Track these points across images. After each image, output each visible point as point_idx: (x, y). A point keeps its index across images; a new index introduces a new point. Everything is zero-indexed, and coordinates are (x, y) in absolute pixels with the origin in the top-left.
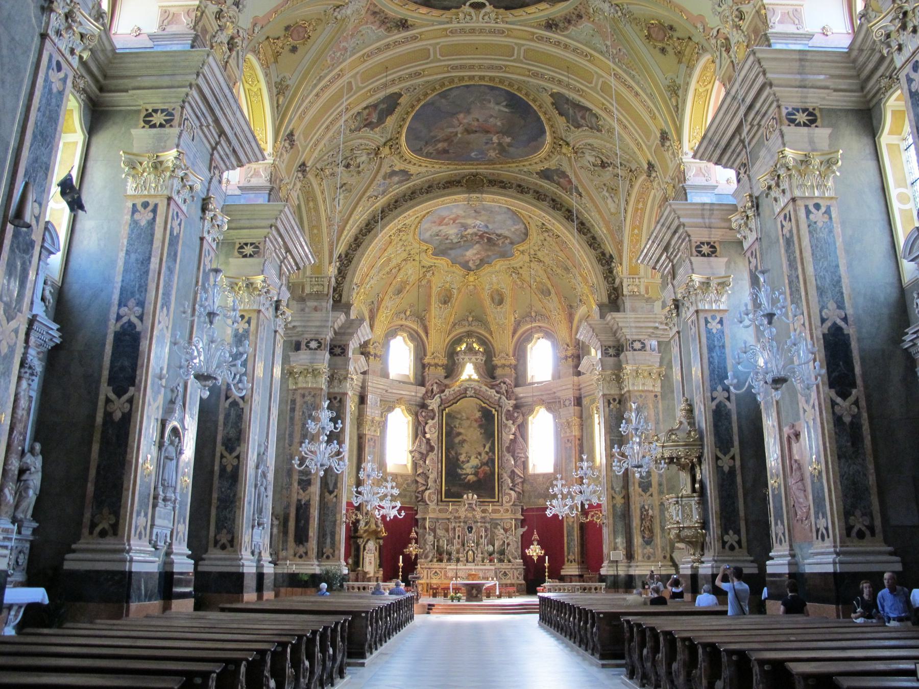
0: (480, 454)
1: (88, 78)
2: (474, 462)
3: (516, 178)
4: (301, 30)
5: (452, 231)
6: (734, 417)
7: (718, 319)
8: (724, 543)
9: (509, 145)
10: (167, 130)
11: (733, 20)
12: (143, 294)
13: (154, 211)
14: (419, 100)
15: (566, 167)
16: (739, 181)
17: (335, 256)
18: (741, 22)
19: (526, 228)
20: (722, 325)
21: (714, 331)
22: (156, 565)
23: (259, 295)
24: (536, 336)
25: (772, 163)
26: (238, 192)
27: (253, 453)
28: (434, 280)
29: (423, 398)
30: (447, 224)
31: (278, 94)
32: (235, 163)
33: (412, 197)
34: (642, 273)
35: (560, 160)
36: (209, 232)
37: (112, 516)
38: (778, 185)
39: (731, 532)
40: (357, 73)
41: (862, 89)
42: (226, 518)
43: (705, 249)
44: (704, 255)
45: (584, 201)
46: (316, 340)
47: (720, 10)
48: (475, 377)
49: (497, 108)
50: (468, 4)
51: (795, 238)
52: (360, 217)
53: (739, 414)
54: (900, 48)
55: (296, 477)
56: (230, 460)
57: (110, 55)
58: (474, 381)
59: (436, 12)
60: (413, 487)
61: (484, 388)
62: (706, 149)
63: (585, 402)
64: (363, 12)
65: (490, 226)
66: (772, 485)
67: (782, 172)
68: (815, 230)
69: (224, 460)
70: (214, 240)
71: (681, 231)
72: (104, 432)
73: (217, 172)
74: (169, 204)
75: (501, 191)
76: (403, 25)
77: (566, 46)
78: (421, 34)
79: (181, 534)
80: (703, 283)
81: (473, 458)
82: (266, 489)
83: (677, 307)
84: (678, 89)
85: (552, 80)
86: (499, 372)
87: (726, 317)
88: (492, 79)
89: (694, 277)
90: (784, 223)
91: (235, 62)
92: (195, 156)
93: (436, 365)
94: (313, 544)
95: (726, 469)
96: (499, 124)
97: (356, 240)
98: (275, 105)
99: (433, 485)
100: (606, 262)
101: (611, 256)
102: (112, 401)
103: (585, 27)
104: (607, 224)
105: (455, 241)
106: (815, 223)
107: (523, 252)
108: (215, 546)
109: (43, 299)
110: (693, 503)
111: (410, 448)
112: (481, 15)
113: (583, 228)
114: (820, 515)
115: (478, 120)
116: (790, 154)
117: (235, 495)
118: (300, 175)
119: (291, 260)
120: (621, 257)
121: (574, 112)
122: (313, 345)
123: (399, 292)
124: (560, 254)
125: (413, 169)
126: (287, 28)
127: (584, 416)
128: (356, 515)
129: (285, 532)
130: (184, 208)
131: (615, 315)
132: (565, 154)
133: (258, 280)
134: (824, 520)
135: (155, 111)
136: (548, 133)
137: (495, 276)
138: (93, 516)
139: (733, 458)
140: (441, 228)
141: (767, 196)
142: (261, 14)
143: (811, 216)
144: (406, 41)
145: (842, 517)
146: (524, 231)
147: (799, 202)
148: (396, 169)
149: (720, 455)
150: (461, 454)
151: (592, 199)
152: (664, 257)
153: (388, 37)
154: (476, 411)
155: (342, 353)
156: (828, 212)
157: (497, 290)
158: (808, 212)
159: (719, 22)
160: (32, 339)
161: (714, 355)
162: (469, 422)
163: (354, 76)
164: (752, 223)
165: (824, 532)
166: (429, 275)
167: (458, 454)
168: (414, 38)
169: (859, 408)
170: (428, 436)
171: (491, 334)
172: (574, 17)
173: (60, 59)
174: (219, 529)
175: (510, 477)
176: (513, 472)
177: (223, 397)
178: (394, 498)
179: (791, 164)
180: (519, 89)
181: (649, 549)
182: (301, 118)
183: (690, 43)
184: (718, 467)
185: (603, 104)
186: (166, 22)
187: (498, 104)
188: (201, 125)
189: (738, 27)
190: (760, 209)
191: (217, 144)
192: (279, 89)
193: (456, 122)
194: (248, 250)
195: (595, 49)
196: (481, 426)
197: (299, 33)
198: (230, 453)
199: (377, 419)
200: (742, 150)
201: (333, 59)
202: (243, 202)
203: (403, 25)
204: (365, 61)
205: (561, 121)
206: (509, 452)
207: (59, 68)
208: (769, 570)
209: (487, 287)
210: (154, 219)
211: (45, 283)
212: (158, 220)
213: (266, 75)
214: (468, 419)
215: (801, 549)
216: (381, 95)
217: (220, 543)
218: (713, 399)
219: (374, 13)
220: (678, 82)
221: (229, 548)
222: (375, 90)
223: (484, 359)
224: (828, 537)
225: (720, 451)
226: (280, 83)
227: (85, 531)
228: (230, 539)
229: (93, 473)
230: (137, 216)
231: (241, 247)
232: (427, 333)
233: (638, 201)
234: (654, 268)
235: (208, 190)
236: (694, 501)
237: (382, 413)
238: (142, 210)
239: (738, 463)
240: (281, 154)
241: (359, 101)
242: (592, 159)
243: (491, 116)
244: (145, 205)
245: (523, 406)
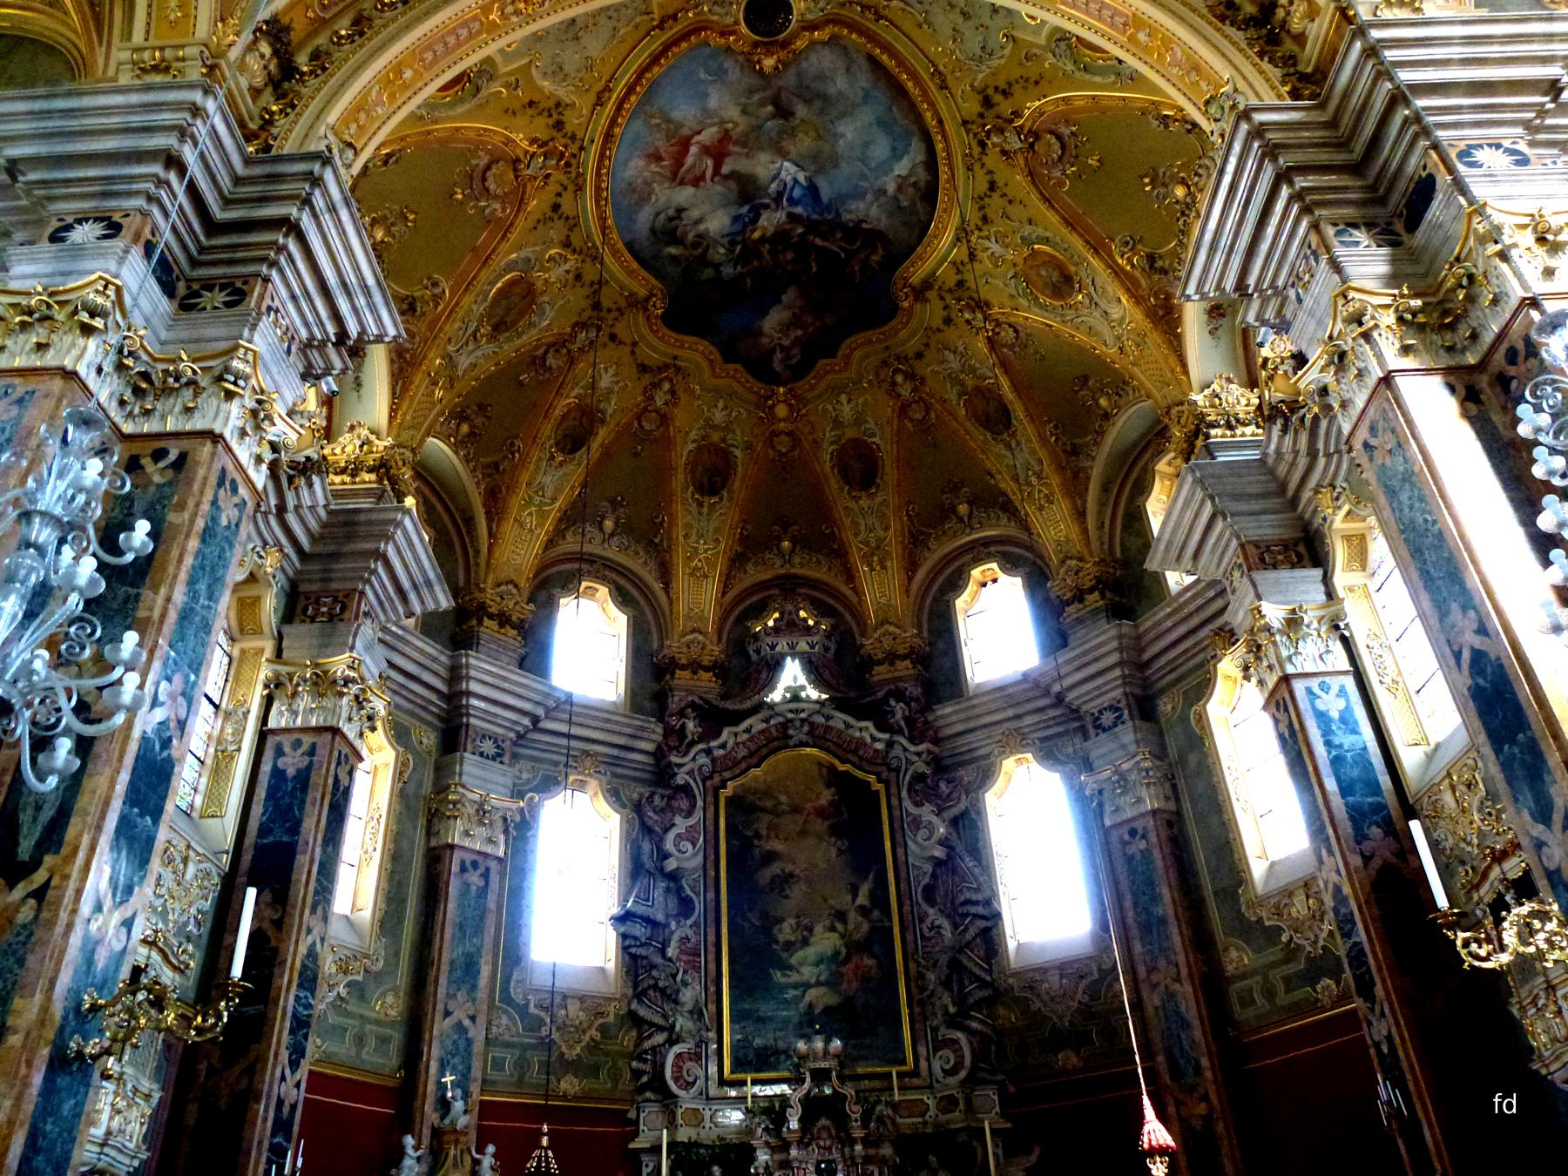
0: (841, 916)
2: (825, 942)
19: (931, 164)
24: (976, 573)
28: (680, 416)
29: (659, 754)
30: (697, 181)
48: (813, 694)
58: (808, 700)
60: (628, 1039)
61: (840, 719)
63: (1165, 706)
65: (826, 193)
81: (818, 929)
86: (881, 673)
93: (695, 666)
99: (689, 1025)
105: (728, 271)
111: (616, 910)
123: (572, 441)
127: (1173, 752)
137: (849, 403)
146: (922, 176)
150: (781, 920)
154: (820, 786)
157: (856, 443)
162: (800, 819)
167: (770, 922)
170: (671, 865)
171: (850, 576)
175: (946, 984)
176: (955, 966)
196: (835, 831)
199: (499, 801)
206: (932, 903)
209: (829, 435)
214: (796, 810)
223: (833, 647)
245: (962, 764)
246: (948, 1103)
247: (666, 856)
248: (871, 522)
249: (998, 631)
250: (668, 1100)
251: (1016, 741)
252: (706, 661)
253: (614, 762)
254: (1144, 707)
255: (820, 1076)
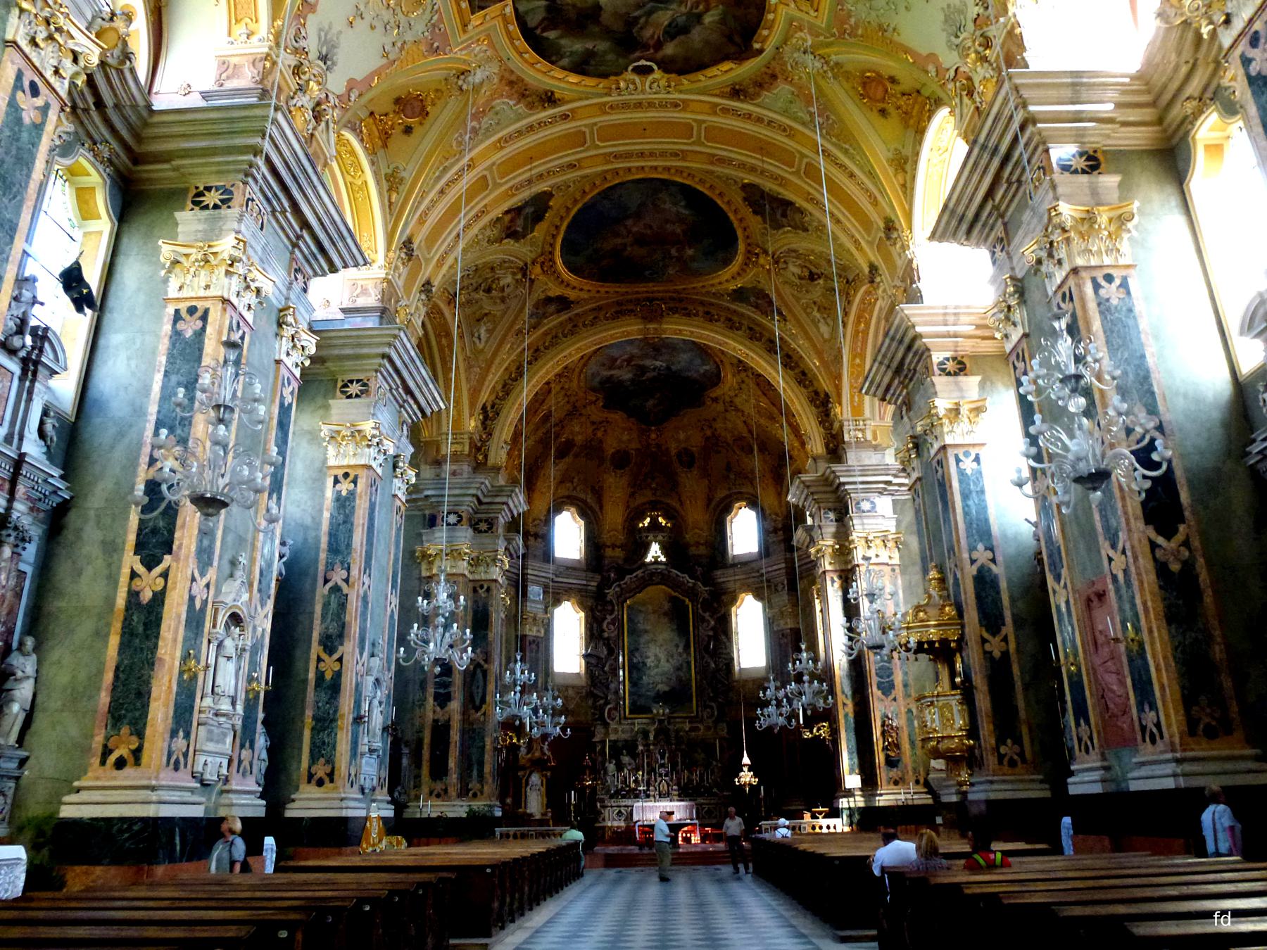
0: (672, 656)
1: (115, 145)
2: (666, 666)
3: (702, 303)
4: (417, 104)
5: (626, 375)
6: (1003, 585)
7: (973, 457)
8: (1001, 758)
9: (693, 259)
10: (224, 211)
11: (977, 52)
12: (186, 429)
13: (204, 318)
14: (576, 201)
15: (764, 284)
16: (994, 263)
17: (479, 406)
18: (987, 52)
20: (979, 463)
21: (969, 472)
22: (202, 808)
23: (369, 446)
25: (1040, 228)
26: (340, 316)
27: (361, 654)
29: (601, 587)
31: (390, 190)
32: (326, 267)
33: (573, 329)
34: (867, 413)
35: (756, 275)
36: (288, 354)
37: (134, 738)
38: (1050, 255)
39: (1009, 741)
40: (494, 164)
41: (1160, 121)
42: (324, 743)
43: (950, 366)
44: (949, 374)
45: (789, 326)
46: (455, 513)
47: (957, 41)
48: (663, 559)
49: (674, 209)
50: (630, 68)
51: (1081, 323)
52: (506, 358)
53: (1009, 581)
54: (1227, 21)
55: (431, 690)
56: (329, 666)
57: (145, 113)
58: (661, 563)
59: (590, 81)
62: (948, 223)
64: (496, 80)
66: (1068, 670)
67: (1057, 237)
68: (1108, 309)
69: (322, 664)
70: (297, 365)
71: (917, 344)
72: (127, 622)
73: (300, 277)
74: (225, 310)
75: (684, 320)
76: (549, 99)
77: (759, 120)
78: (572, 110)
79: (246, 763)
80: (950, 410)
82: (380, 703)
83: (916, 446)
84: (905, 163)
85: (742, 166)
87: (983, 453)
88: (668, 169)
89: (938, 402)
90: (1062, 305)
91: (324, 137)
92: (264, 249)
94: (453, 777)
95: (997, 654)
96: (679, 231)
97: (504, 387)
98: (387, 203)
100: (823, 404)
101: (827, 395)
102: (139, 576)
103: (782, 90)
104: (819, 354)
106: (1108, 300)
107: (715, 400)
108: (309, 782)
109: (42, 433)
110: (954, 703)
112: (648, 84)
113: (790, 361)
114: (1147, 708)
115: (651, 227)
116: (1067, 211)
117: (336, 712)
118: (423, 297)
119: (415, 407)
120: (839, 395)
121: (776, 210)
122: (453, 519)
124: (763, 398)
125: (572, 295)
126: (398, 101)
128: (511, 738)
129: (418, 765)
130: (249, 317)
131: (837, 468)
132: (763, 266)
133: (368, 427)
134: (1153, 714)
135: (208, 189)
136: (740, 241)
137: (682, 434)
138: (107, 739)
139: (1005, 639)
140: (612, 372)
141: (1035, 274)
142: (359, 76)
143: (1102, 292)
144: (554, 120)
145: (1181, 708)
147: (1083, 274)
148: (551, 294)
149: (986, 635)
151: (798, 321)
152: (896, 382)
153: (531, 115)
155: (490, 529)
156: (1124, 285)
158: (1097, 286)
159: (957, 59)
160: (21, 490)
161: (970, 503)
163: (490, 168)
164: (1017, 315)
165: (1155, 730)
166: (599, 434)
168: (565, 117)
169: (1190, 551)
170: (606, 635)
171: (682, 504)
172: (767, 79)
173: (37, 79)
174: (313, 759)
177: (320, 581)
178: (556, 713)
179: (1068, 224)
180: (702, 181)
181: (894, 773)
182: (421, 221)
183: (920, 99)
184: (985, 652)
185: (809, 194)
186: (224, 76)
187: (675, 204)
188: (274, 211)
189: (984, 59)
190: (1026, 296)
191: (299, 237)
192: (391, 182)
193: (623, 231)
194: (354, 389)
195: (795, 119)
196: (671, 620)
197: (413, 108)
198: (330, 655)
199: (541, 615)
200: (996, 220)
201: (459, 144)
202: (346, 327)
203: (549, 99)
204: (502, 148)
205: (755, 222)
207: (35, 91)
208: (1073, 790)
210: (204, 329)
211: (45, 413)
212: (209, 329)
213: (373, 163)
215: (1119, 758)
216: (525, 194)
217: (316, 777)
218: (973, 562)
219: (511, 83)
220: (904, 152)
221: (328, 785)
222: (517, 188)
224: (1162, 737)
225: (987, 631)
226: (392, 175)
227: (96, 761)
228: (328, 771)
229: (109, 677)
230: (180, 326)
231: (345, 386)
232: (601, 507)
233: (858, 322)
234: (883, 399)
235: (287, 299)
236: (954, 701)
237: (546, 607)
238: (188, 317)
239: (1012, 646)
240: (396, 268)
241: (498, 202)
242: (797, 271)
243: (667, 221)
244: (192, 310)
246: (708, 728)
247: (603, 631)
248: (691, 483)
249: (744, 533)
250: (606, 725)
251: (748, 588)
252: (618, 543)
253: (580, 591)
254: (792, 588)
255: (661, 722)
